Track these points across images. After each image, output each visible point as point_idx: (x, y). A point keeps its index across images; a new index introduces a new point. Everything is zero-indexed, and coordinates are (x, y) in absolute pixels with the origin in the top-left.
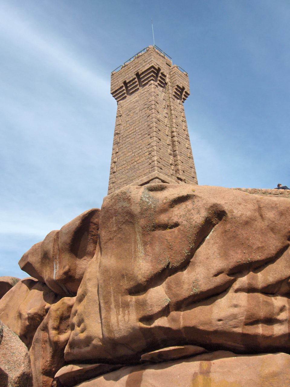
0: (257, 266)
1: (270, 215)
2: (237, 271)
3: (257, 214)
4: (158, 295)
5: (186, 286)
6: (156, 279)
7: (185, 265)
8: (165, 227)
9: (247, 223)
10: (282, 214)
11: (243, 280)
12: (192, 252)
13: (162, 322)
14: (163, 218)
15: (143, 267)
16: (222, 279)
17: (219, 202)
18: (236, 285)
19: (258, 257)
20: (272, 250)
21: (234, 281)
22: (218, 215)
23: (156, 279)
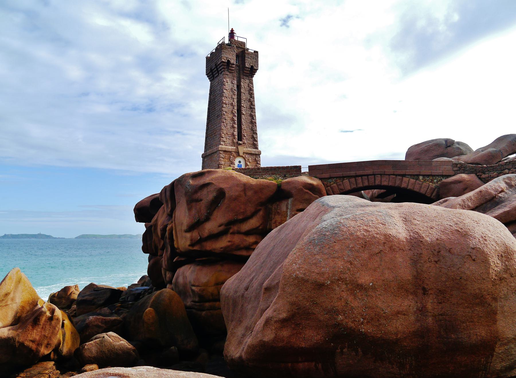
3: (242, 193)
4: (195, 234)
5: (207, 231)
7: (207, 219)
9: (236, 199)
10: (256, 192)
11: (235, 228)
17: (223, 187)
18: (231, 231)
20: (249, 213)
21: (230, 228)
22: (221, 194)
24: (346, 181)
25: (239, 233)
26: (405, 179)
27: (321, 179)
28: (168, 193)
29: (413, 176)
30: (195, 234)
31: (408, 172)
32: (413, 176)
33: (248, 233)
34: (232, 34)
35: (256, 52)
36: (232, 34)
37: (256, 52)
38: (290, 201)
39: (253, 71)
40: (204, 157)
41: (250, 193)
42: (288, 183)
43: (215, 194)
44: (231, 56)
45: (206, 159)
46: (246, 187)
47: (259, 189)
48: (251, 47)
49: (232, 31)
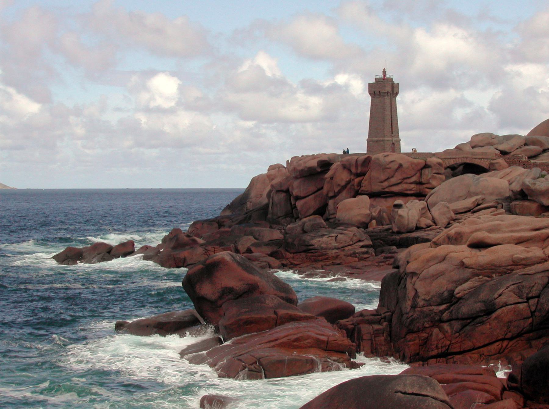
0: (409, 178)
1: (413, 166)
2: (404, 179)
4: (386, 184)
6: (385, 180)
7: (392, 177)
8: (388, 168)
11: (405, 181)
12: (394, 174)
13: (386, 190)
14: (388, 166)
15: (383, 177)
16: (400, 181)
19: (409, 176)
22: (401, 166)
23: (385, 180)
24: (452, 160)
25: (407, 183)
26: (477, 160)
27: (441, 159)
28: (359, 163)
29: (479, 159)
30: (386, 184)
31: (478, 157)
32: (479, 159)
33: (411, 183)
34: (384, 72)
35: (398, 84)
36: (384, 72)
37: (398, 84)
38: (430, 169)
39: (397, 94)
40: (367, 140)
41: (413, 166)
42: (430, 161)
43: (397, 166)
44: (388, 89)
45: (371, 143)
46: (412, 163)
47: (417, 164)
48: (395, 81)
49: (384, 69)
